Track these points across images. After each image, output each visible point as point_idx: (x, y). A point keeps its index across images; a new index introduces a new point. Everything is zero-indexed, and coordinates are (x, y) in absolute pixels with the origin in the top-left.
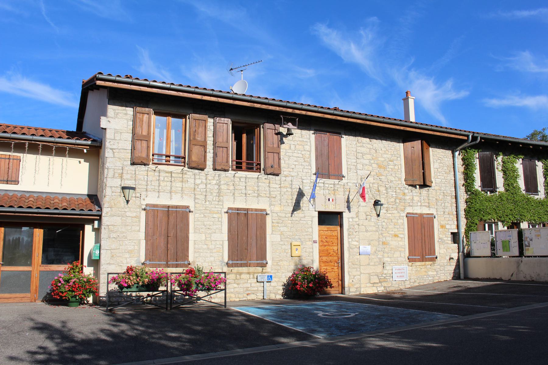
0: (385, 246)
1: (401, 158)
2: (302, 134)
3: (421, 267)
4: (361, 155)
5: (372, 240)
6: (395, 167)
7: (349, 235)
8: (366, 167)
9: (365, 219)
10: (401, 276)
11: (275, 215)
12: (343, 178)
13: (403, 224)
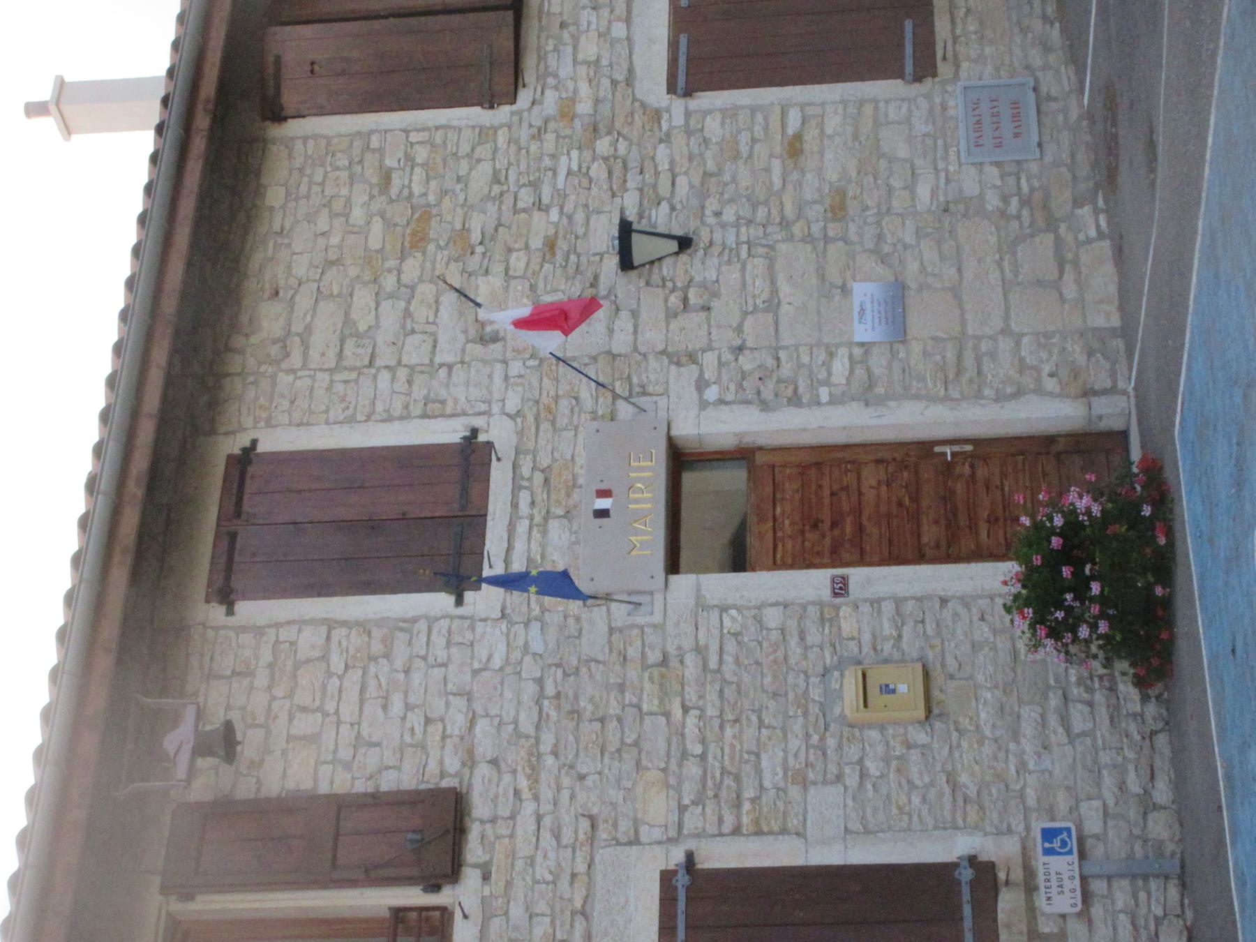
0: (853, 207)
1: (371, 132)
2: (235, 673)
3: (961, 13)
4: (350, 344)
5: (822, 277)
6: (419, 160)
7: (795, 401)
8: (421, 313)
9: (706, 313)
10: (1016, 117)
11: (692, 821)
12: (482, 438)
13: (729, 114)
